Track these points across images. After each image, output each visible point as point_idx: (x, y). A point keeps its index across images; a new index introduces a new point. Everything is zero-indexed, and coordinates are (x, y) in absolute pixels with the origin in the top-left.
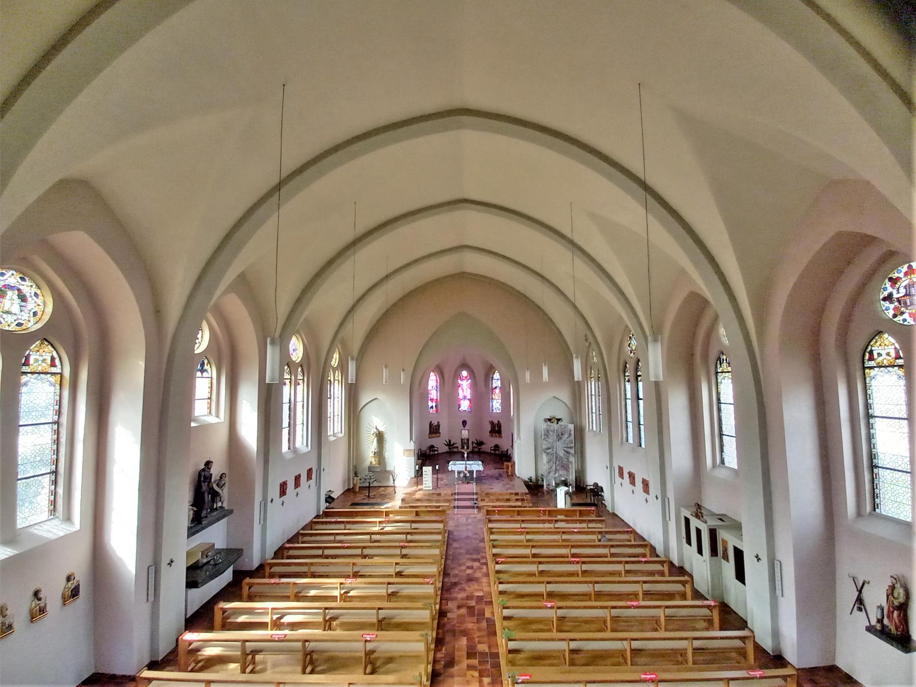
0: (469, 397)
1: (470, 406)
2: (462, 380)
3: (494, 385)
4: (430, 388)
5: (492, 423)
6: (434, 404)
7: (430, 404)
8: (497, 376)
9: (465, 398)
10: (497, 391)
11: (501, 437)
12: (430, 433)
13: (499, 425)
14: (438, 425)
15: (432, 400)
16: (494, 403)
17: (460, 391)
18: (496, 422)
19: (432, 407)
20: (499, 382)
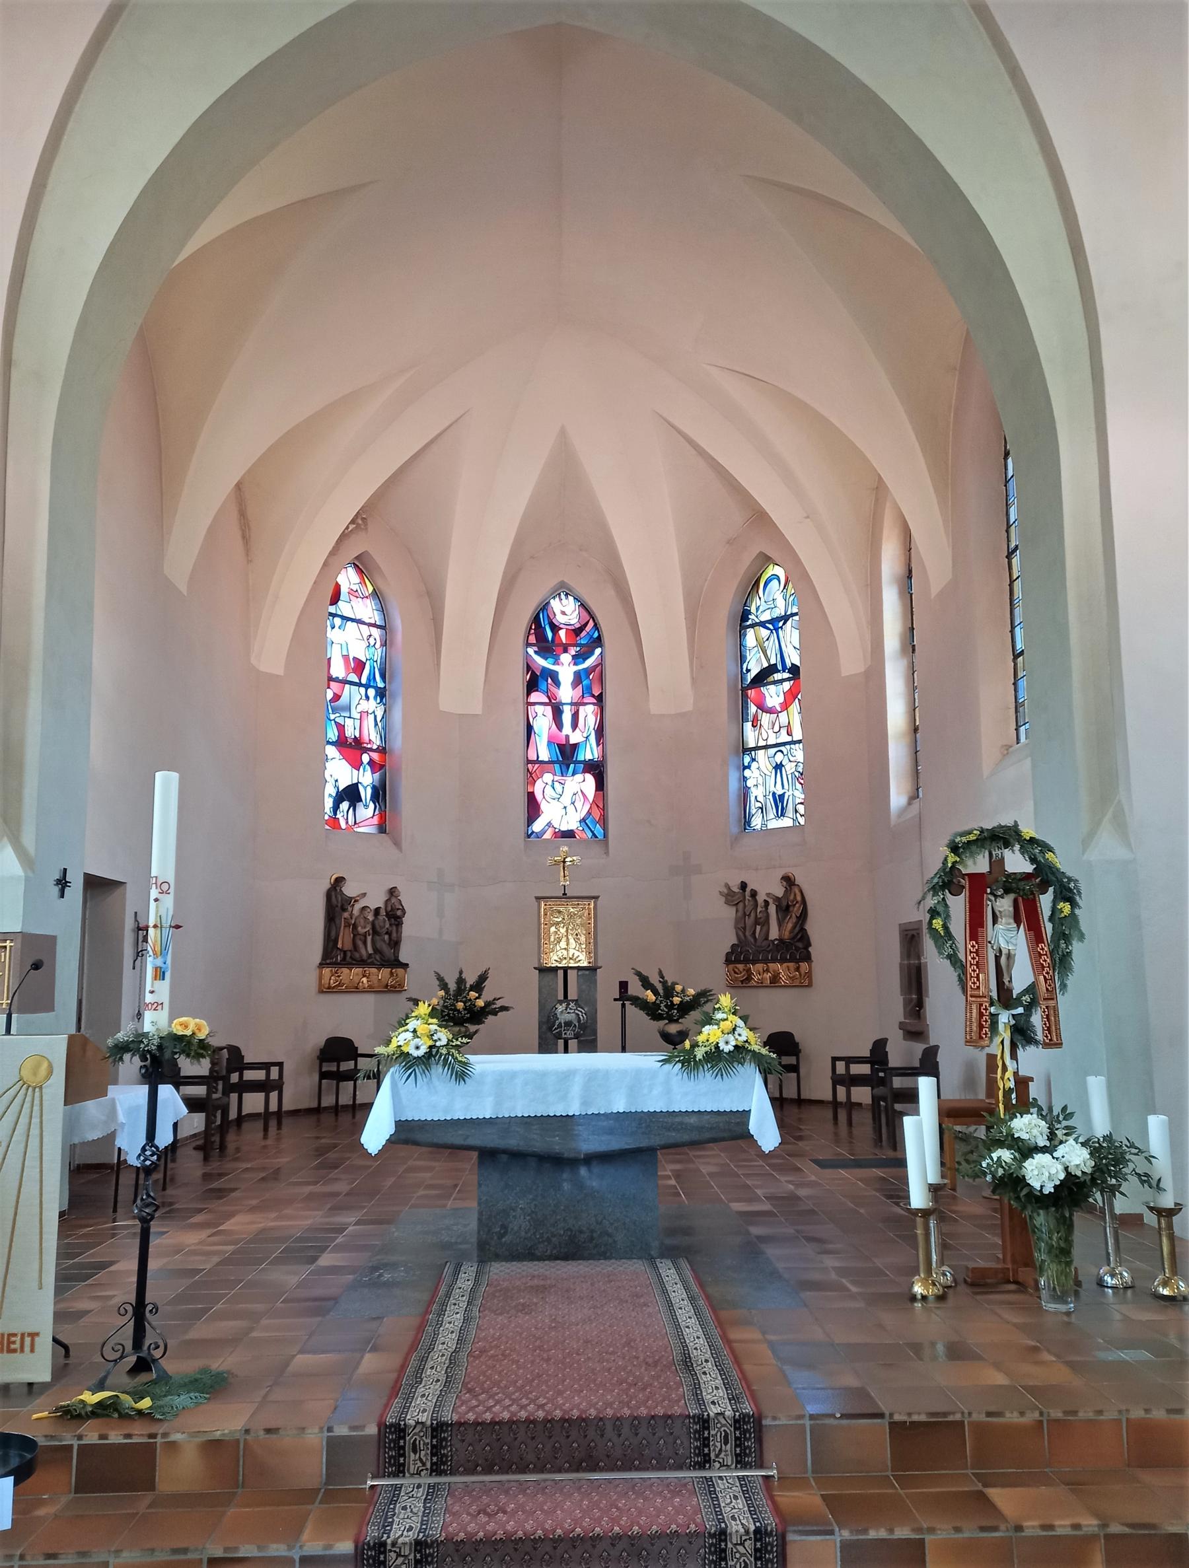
0: (590, 752)
2: (548, 648)
3: (754, 666)
5: (741, 897)
6: (367, 779)
7: (339, 772)
8: (772, 600)
9: (566, 754)
10: (773, 695)
11: (805, 982)
12: (334, 955)
13: (792, 904)
14: (393, 914)
15: (352, 748)
17: (543, 721)
18: (769, 886)
19: (351, 794)
20: (791, 635)
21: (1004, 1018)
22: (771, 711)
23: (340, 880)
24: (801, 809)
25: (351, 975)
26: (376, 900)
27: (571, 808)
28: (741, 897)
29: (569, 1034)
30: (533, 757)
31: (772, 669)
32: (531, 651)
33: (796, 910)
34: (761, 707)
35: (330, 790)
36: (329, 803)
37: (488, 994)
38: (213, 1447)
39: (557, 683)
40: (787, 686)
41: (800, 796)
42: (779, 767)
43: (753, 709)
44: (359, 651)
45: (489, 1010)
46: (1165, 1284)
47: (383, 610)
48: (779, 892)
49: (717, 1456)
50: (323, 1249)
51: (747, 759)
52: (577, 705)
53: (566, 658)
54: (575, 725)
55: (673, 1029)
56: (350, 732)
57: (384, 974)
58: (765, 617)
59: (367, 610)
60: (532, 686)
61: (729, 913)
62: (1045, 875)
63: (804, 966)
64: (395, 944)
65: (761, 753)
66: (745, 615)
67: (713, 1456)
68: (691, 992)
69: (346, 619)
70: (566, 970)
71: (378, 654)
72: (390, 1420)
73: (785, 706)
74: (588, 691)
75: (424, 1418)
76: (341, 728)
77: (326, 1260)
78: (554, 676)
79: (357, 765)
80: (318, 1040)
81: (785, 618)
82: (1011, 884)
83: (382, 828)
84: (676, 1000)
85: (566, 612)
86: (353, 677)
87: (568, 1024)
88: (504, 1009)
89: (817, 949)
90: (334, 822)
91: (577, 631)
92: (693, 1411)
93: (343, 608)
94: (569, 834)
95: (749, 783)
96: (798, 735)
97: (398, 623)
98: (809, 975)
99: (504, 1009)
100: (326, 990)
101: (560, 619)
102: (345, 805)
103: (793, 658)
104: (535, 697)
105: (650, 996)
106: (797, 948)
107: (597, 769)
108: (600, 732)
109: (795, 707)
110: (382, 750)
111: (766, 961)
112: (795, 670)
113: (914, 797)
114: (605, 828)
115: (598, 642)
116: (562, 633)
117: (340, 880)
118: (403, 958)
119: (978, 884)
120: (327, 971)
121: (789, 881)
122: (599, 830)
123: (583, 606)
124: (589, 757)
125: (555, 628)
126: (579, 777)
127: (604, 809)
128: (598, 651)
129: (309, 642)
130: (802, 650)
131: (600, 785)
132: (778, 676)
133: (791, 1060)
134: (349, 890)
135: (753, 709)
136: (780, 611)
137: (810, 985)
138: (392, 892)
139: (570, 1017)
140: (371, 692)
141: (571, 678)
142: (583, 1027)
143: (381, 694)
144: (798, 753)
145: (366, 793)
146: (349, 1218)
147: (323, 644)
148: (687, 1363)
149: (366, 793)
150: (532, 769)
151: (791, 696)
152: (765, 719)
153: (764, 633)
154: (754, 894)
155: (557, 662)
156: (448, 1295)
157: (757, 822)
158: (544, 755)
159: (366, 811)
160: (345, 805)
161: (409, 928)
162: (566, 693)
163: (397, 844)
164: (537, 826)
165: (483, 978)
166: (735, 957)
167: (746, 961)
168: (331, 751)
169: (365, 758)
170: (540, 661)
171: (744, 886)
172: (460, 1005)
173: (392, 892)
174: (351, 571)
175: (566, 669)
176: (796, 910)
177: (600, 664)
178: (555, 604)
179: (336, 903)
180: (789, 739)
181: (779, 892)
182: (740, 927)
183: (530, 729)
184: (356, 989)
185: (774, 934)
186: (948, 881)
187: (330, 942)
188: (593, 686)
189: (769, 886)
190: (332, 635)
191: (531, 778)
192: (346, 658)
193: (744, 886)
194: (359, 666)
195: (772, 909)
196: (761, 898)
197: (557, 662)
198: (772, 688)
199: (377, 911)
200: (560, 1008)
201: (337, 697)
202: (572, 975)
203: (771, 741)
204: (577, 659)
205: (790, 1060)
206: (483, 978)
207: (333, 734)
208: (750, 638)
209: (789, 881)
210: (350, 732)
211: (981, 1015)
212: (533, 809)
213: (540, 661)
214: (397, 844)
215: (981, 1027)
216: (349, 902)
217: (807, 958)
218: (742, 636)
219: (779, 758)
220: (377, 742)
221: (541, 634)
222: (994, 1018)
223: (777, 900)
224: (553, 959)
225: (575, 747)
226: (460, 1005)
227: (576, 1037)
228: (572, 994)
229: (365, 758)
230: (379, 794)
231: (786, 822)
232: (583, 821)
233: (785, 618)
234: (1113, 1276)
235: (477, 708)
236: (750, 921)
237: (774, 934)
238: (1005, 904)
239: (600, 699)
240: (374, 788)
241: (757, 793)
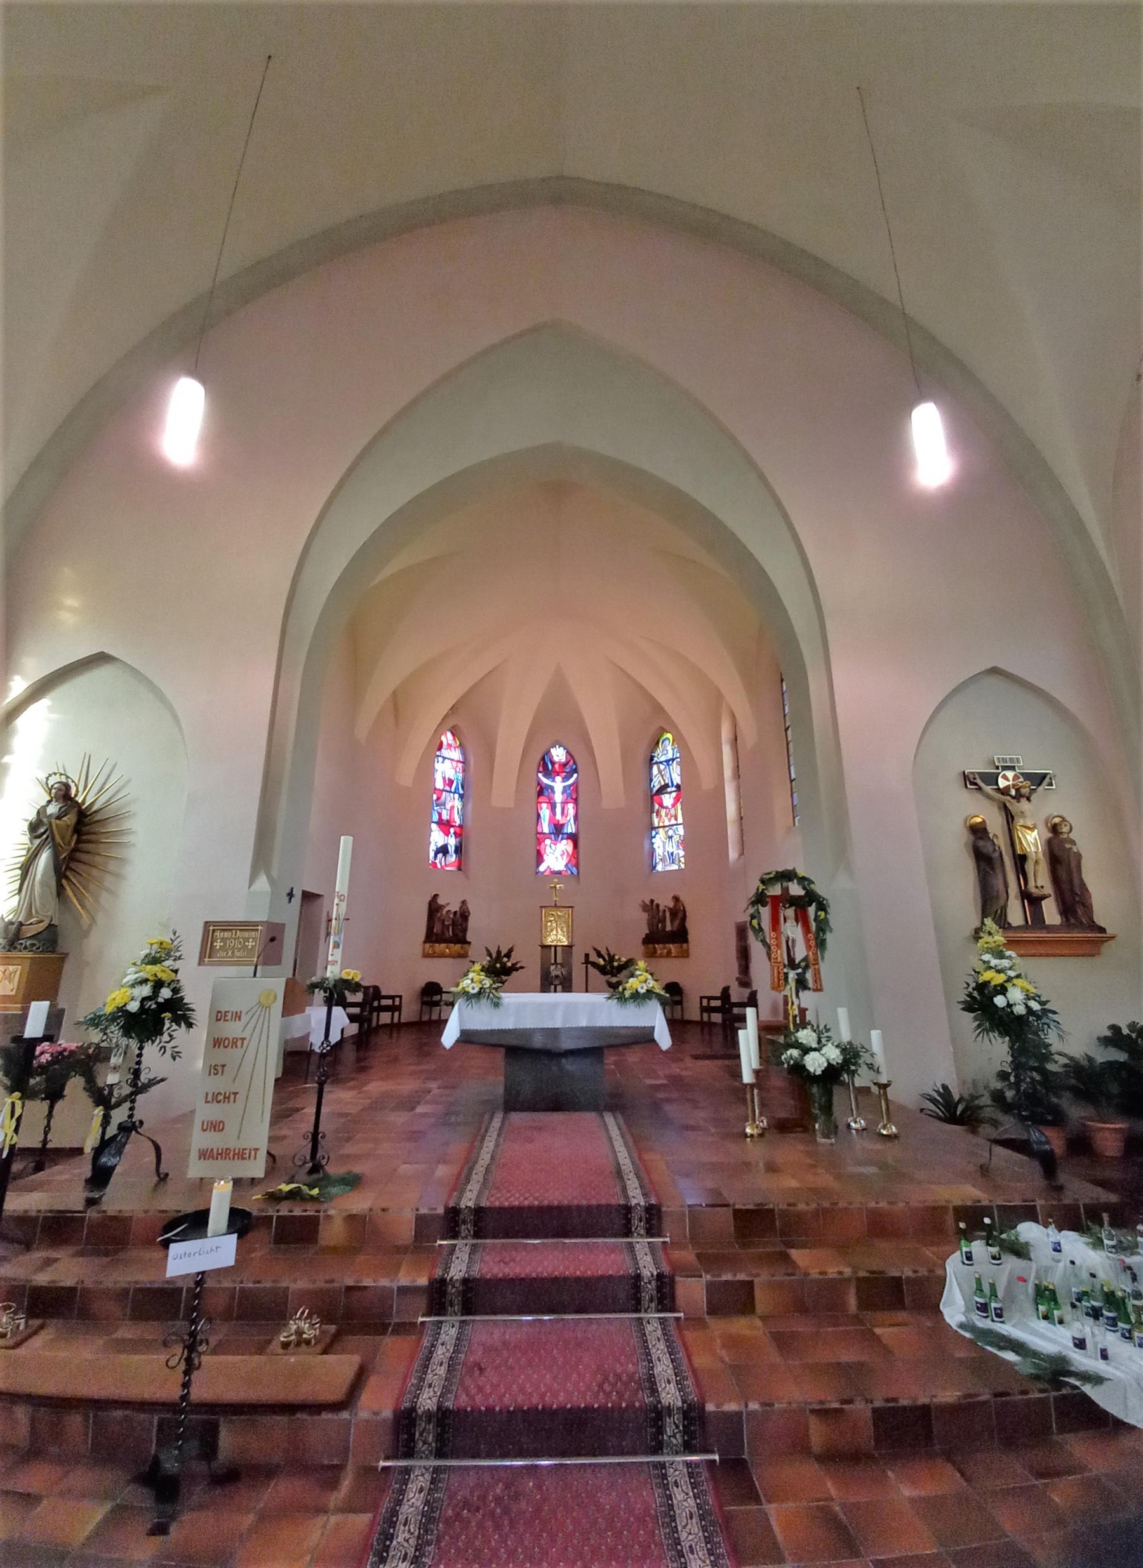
0: (570, 828)
1: (575, 858)
2: (548, 774)
3: (657, 783)
4: (439, 785)
5: (651, 908)
6: (452, 842)
7: (437, 838)
8: (667, 750)
9: (558, 829)
10: (668, 800)
11: (685, 954)
13: (678, 912)
14: (463, 915)
15: (445, 825)
16: (659, 841)
17: (545, 812)
18: (665, 902)
19: (444, 850)
21: (792, 975)
22: (666, 808)
23: (436, 896)
24: (682, 860)
25: (440, 947)
26: (455, 907)
27: (560, 858)
28: (651, 908)
29: (557, 982)
30: (540, 830)
31: (667, 786)
32: (540, 775)
33: (680, 915)
34: (661, 805)
35: (433, 848)
36: (432, 854)
37: (513, 960)
38: (351, 1218)
39: (553, 792)
40: (674, 794)
41: (682, 853)
42: (671, 837)
43: (657, 807)
44: (450, 774)
45: (514, 968)
46: (884, 1127)
47: (464, 754)
48: (671, 905)
49: (684, 1527)
50: (419, 1103)
51: (654, 833)
52: (564, 803)
53: (558, 779)
54: (563, 814)
55: (614, 980)
56: (445, 817)
57: (457, 947)
58: (663, 759)
59: (456, 755)
60: (540, 793)
61: (645, 916)
62: (811, 897)
63: (685, 945)
64: (465, 930)
65: (661, 830)
66: (652, 758)
67: (680, 1528)
68: (624, 959)
69: (444, 758)
70: (556, 947)
71: (460, 776)
72: (451, 1204)
73: (674, 805)
74: (570, 796)
75: (471, 1204)
76: (440, 814)
77: (419, 1109)
78: (552, 788)
79: (447, 834)
80: (421, 983)
81: (673, 760)
82: (794, 901)
83: (459, 869)
84: (616, 964)
85: (559, 754)
86: (447, 788)
87: (557, 976)
88: (522, 968)
89: (691, 937)
90: (434, 864)
91: (564, 765)
92: (622, 1202)
93: (445, 752)
94: (559, 873)
95: (655, 846)
96: (680, 820)
97: (472, 761)
98: (688, 950)
99: (522, 968)
100: (426, 955)
101: (556, 759)
102: (440, 855)
103: (677, 780)
104: (541, 799)
105: (602, 962)
106: (680, 936)
107: (574, 838)
108: (576, 817)
109: (679, 806)
110: (461, 826)
111: (664, 943)
112: (678, 787)
113: (742, 853)
114: (578, 869)
115: (575, 771)
116: (557, 766)
117: (436, 896)
118: (468, 939)
119: (776, 903)
120: (428, 945)
121: (676, 899)
122: (574, 870)
123: (568, 753)
124: (569, 831)
125: (553, 763)
126: (565, 841)
127: (577, 859)
128: (575, 775)
129: (426, 770)
130: (682, 776)
131: (576, 846)
132: (669, 790)
133: (677, 998)
134: (441, 901)
135: (657, 807)
136: (670, 756)
137: (688, 956)
138: (464, 902)
139: (558, 973)
140: (457, 796)
141: (561, 789)
142: (564, 978)
143: (461, 796)
144: (681, 830)
145: (452, 849)
146: (433, 1085)
147: (434, 770)
148: (619, 1173)
149: (452, 849)
150: (540, 838)
151: (677, 799)
152: (663, 812)
153: (662, 767)
154: (658, 905)
155: (554, 781)
156: (486, 1131)
157: (659, 868)
158: (546, 830)
159: (452, 858)
160: (440, 855)
161: (472, 923)
162: (558, 797)
163: (467, 877)
164: (542, 868)
165: (511, 950)
166: (649, 940)
167: (653, 943)
168: (434, 826)
169: (452, 830)
170: (545, 781)
171: (652, 901)
172: (498, 965)
173: (464, 902)
174: (449, 734)
175: (558, 785)
176: (680, 915)
177: (575, 784)
178: (553, 751)
179: (434, 908)
180: (673, 822)
181: (671, 905)
182: (650, 924)
183: (539, 816)
184: (442, 955)
185: (668, 928)
186: (760, 899)
187: (430, 928)
188: (573, 795)
189: (665, 902)
190: (437, 766)
191: (540, 842)
192: (444, 778)
193: (652, 901)
194: (451, 782)
195: (668, 914)
196: (661, 908)
197: (554, 781)
198: (667, 796)
199: (455, 913)
200: (552, 967)
201: (438, 798)
202: (559, 950)
203: (667, 823)
204: (565, 779)
205: (677, 998)
206: (511, 950)
207: (435, 818)
208: (655, 769)
209: (676, 899)
210: (445, 817)
211: (779, 973)
212: (540, 858)
213: (545, 781)
214: (467, 877)
215: (779, 980)
216: (441, 907)
217: (686, 941)
218: (651, 768)
219: (670, 833)
220: (458, 822)
221: (546, 766)
222: (786, 974)
223: (670, 909)
224: (549, 941)
225: (563, 825)
226: (498, 965)
227: (561, 984)
228: (559, 961)
229: (452, 830)
230: (458, 850)
231: (675, 867)
232: (566, 865)
233: (673, 760)
234: (855, 1122)
235: (511, 804)
236: (656, 921)
237: (668, 928)
238: (790, 912)
239: (576, 801)
240: (456, 847)
241: (659, 851)
